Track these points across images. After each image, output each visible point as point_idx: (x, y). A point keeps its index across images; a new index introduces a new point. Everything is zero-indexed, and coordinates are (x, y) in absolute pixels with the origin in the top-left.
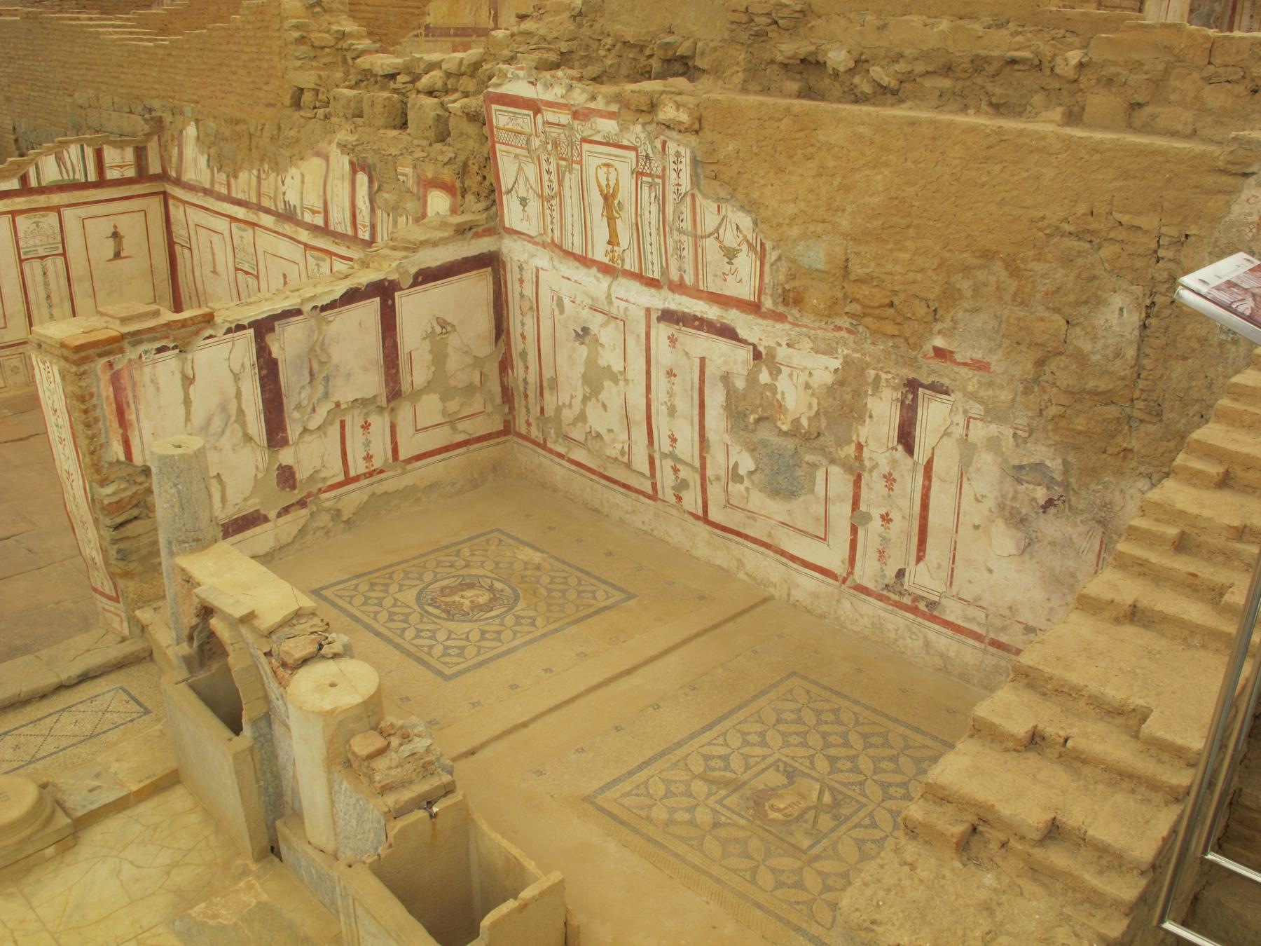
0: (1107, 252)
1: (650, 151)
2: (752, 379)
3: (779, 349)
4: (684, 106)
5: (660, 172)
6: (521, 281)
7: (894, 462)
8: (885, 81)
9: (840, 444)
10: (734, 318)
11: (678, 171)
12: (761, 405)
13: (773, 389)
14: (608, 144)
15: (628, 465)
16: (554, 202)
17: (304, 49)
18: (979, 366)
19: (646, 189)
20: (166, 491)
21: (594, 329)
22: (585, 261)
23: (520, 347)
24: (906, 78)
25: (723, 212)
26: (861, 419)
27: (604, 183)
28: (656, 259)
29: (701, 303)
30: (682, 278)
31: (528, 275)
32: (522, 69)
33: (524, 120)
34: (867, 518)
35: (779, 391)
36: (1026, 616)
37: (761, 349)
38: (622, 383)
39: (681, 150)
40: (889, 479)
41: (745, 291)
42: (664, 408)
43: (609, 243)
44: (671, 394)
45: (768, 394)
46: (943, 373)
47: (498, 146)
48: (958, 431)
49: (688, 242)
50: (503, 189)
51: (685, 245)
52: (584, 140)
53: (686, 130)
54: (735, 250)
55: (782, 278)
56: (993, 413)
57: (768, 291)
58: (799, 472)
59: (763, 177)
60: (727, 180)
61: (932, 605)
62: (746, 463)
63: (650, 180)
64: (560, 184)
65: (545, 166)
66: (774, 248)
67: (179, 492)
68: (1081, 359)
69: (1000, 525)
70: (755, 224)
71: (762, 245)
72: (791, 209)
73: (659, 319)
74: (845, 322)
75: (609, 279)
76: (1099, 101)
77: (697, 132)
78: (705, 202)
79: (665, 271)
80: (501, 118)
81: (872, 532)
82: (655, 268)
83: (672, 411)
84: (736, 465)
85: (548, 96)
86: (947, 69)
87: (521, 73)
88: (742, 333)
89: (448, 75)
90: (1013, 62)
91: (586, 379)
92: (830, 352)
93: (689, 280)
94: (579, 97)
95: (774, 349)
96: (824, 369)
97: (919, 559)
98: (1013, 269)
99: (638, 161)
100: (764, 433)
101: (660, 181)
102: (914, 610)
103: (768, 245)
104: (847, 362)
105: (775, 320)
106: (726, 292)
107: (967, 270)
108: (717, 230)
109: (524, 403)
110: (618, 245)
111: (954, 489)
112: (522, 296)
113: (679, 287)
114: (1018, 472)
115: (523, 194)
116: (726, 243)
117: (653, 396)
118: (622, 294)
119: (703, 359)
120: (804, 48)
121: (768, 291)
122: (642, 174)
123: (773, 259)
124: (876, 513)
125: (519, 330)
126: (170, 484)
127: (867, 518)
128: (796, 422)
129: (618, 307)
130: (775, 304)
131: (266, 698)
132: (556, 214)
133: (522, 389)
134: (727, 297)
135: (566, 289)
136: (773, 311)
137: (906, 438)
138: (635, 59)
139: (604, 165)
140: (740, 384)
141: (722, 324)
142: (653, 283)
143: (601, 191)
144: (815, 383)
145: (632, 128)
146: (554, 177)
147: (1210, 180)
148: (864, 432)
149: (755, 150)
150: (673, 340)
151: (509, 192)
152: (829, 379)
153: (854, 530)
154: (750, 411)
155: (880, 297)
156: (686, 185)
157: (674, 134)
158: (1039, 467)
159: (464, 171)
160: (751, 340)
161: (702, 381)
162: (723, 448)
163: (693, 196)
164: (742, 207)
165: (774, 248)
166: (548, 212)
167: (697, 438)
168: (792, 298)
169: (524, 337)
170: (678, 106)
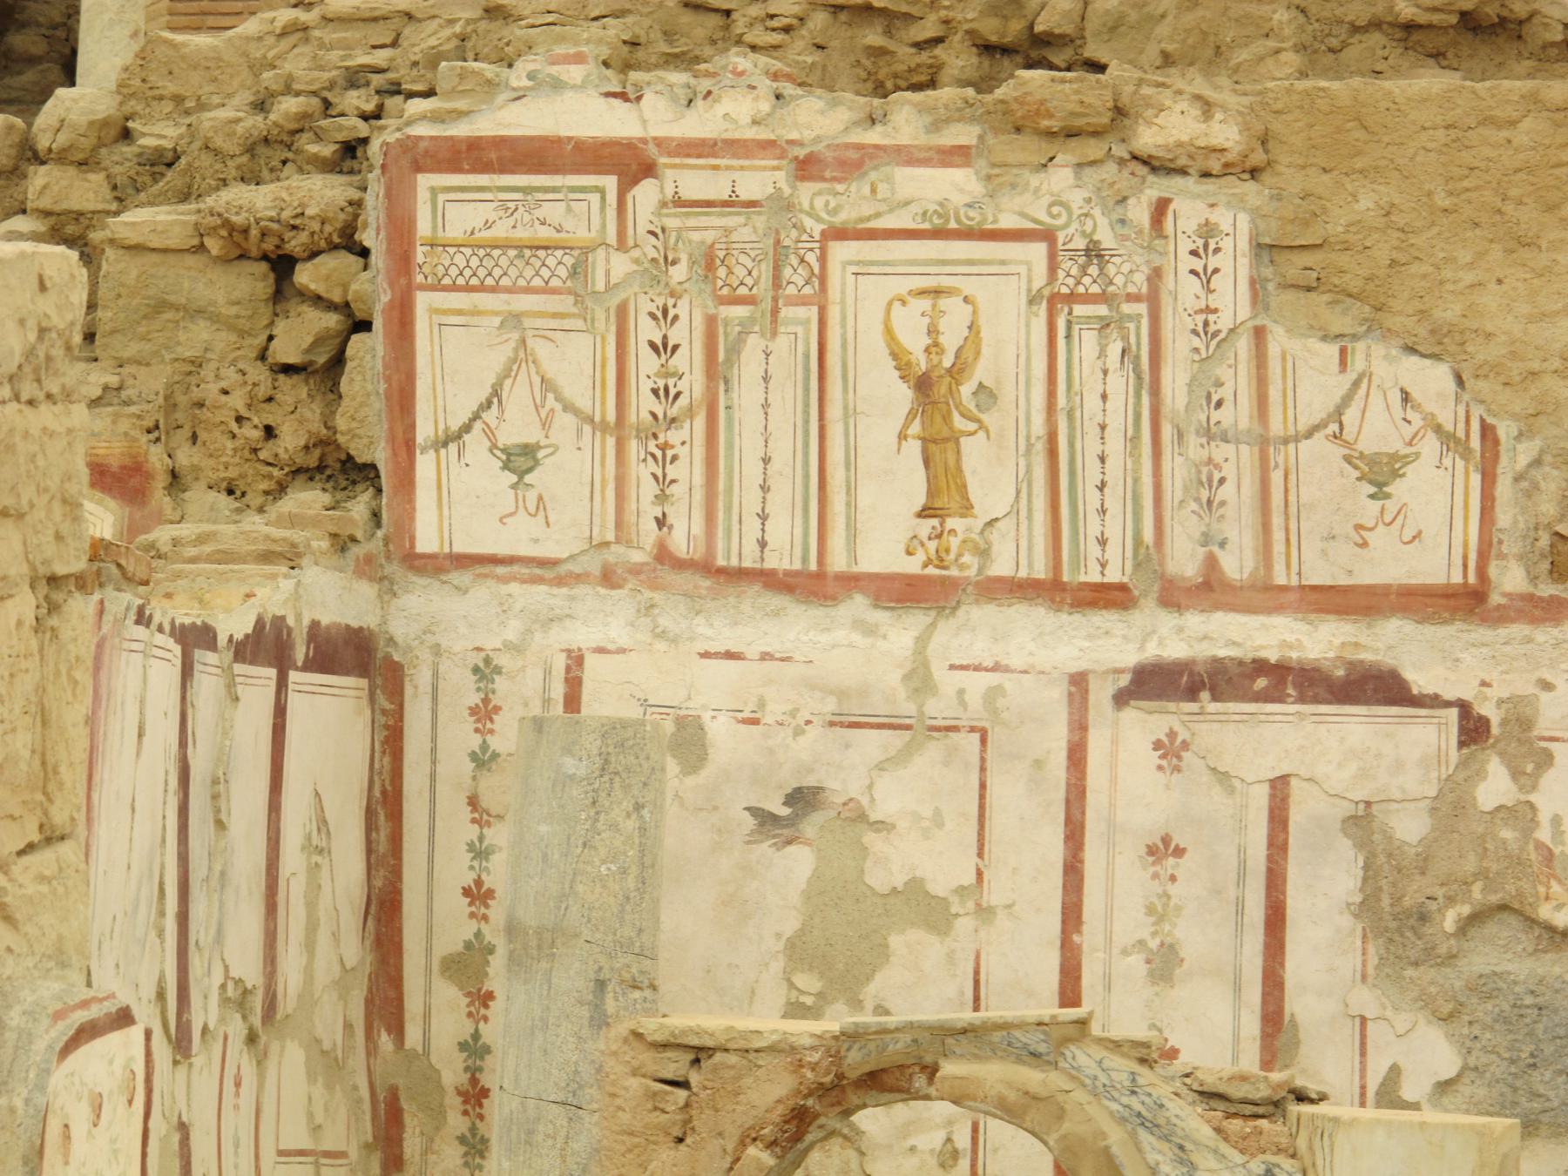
1: (1106, 238)
3: (1545, 697)
4: (1225, 109)
5: (1140, 282)
6: (484, 713)
10: (1394, 643)
11: (1206, 277)
12: (1482, 874)
13: (1522, 815)
14: (938, 234)
16: (674, 436)
19: (1088, 341)
20: (614, 827)
22: (813, 585)
25: (1358, 364)
27: (914, 342)
29: (1279, 621)
30: (1211, 563)
31: (525, 690)
32: (579, 59)
33: (576, 208)
35: (1544, 817)
37: (1487, 710)
38: (964, 925)
39: (1232, 218)
41: (1436, 564)
42: (1136, 962)
43: (925, 512)
44: (1159, 913)
45: (1507, 834)
47: (422, 301)
49: (1237, 462)
50: (424, 430)
51: (1229, 471)
52: (841, 234)
53: (1228, 169)
54: (1394, 457)
55: (1548, 508)
57: (1511, 547)
59: (1471, 266)
60: (1354, 285)
62: (1430, 1054)
63: (1102, 310)
64: (716, 371)
66: (1520, 436)
67: (643, 830)
70: (1460, 381)
71: (1487, 431)
73: (1122, 699)
75: (916, 620)
77: (1254, 173)
78: (1295, 346)
79: (1147, 555)
80: (451, 210)
82: (1113, 552)
83: (1164, 964)
84: (1394, 1072)
85: (699, 124)
87: (575, 73)
88: (1420, 680)
91: (798, 951)
93: (1236, 564)
94: (820, 119)
95: (1530, 700)
99: (1053, 267)
101: (1142, 308)
103: (1505, 430)
105: (1534, 621)
106: (1368, 576)
108: (1338, 414)
109: (456, 1122)
110: (967, 509)
113: (1209, 589)
116: (1368, 445)
117: (1090, 937)
118: (979, 648)
119: (1280, 788)
121: (1511, 547)
122: (1072, 298)
123: (1523, 460)
125: (456, 871)
126: (628, 805)
130: (1533, 579)
132: (687, 471)
134: (1370, 590)
135: (711, 692)
136: (1530, 598)
138: (878, 53)
139: (922, 293)
140: (1410, 827)
141: (1351, 665)
142: (1109, 597)
143: (903, 365)
145: (1034, 180)
149: (1442, 200)
150: (1170, 751)
151: (454, 438)
156: (1232, 301)
157: (1190, 183)
159: (177, 417)
160: (1449, 695)
161: (1278, 846)
162: (1350, 1031)
163: (1259, 334)
164: (1411, 350)
165: (1520, 436)
166: (642, 474)
167: (1251, 1025)
169: (477, 894)
170: (1207, 107)
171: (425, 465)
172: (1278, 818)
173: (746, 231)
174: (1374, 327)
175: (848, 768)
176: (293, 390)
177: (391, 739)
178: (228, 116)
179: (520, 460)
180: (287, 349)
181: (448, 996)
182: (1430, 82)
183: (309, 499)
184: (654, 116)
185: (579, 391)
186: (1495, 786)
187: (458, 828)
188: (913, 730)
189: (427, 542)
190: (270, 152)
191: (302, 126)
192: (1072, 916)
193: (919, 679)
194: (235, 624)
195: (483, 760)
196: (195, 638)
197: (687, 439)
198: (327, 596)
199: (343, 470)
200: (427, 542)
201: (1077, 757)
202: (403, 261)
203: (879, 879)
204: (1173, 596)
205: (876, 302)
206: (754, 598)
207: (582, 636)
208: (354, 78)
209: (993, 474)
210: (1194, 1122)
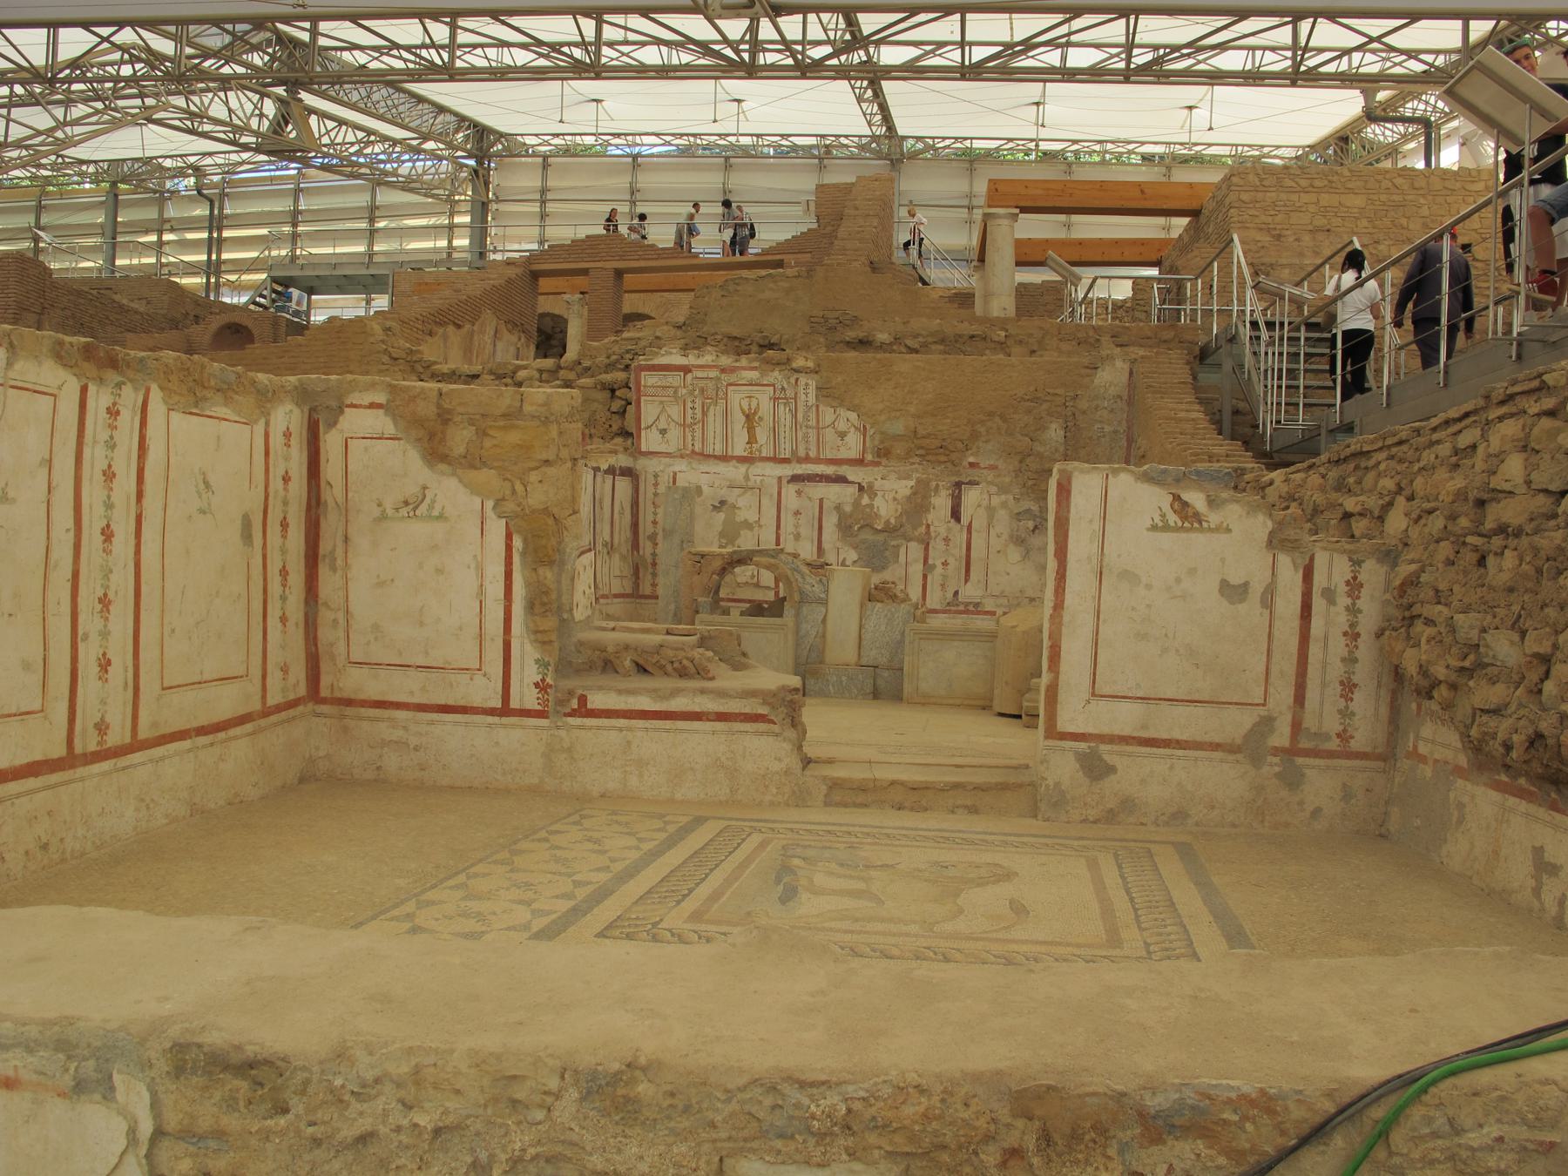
0: (1045, 406)
2: (856, 504)
6: (656, 485)
7: (949, 530)
8: (916, 346)
9: (915, 528)
13: (871, 506)
15: (757, 585)
17: (386, 359)
18: (993, 468)
21: (731, 500)
22: (724, 458)
23: (650, 530)
24: (925, 345)
26: (928, 511)
27: (746, 408)
28: (788, 446)
31: (665, 480)
33: (674, 379)
34: (934, 567)
36: (1029, 593)
40: (947, 540)
41: (853, 454)
46: (974, 474)
48: (985, 503)
49: (812, 434)
56: (1003, 490)
58: (887, 553)
61: (977, 605)
62: (852, 555)
64: (704, 413)
65: (689, 405)
68: (1040, 456)
69: (1011, 546)
72: (881, 406)
74: (917, 460)
76: (1016, 350)
79: (794, 452)
80: (649, 379)
81: (935, 578)
83: (797, 537)
85: (700, 362)
86: (943, 341)
88: (850, 478)
89: (541, 371)
90: (972, 337)
91: (722, 535)
92: (908, 477)
93: (812, 454)
94: (726, 361)
96: (904, 488)
97: (966, 581)
98: (1005, 420)
100: (867, 535)
102: (966, 612)
104: (919, 481)
107: (982, 422)
111: (985, 535)
112: (656, 494)
113: (807, 459)
114: (1018, 516)
115: (662, 425)
117: (782, 531)
118: (759, 471)
119: (821, 501)
120: (861, 335)
124: (938, 563)
125: (650, 518)
127: (934, 567)
128: (888, 522)
129: (755, 480)
131: (801, 593)
132: (698, 434)
133: (649, 560)
135: (704, 481)
137: (956, 514)
140: (848, 509)
142: (785, 461)
144: (899, 496)
146: (699, 411)
147: (1084, 371)
148: (931, 517)
150: (799, 493)
152: (908, 492)
153: (925, 577)
154: (853, 525)
155: (938, 443)
156: (812, 399)
158: (1028, 511)
161: (821, 512)
166: (689, 435)
168: (883, 453)
169: (655, 523)
171: (643, 433)
172: (821, 507)
173: (710, 384)
174: (841, 405)
175: (732, 496)
176: (615, 417)
177: (636, 490)
178: (602, 359)
179: (663, 432)
180: (614, 409)
181: (649, 544)
182: (852, 354)
183: (619, 440)
184: (691, 360)
185: (675, 418)
186: (865, 500)
187: (651, 509)
188: (746, 489)
189: (644, 449)
190: (610, 367)
191: (617, 361)
192: (778, 527)
193: (747, 478)
194: (604, 467)
195: (656, 494)
196: (596, 469)
197: (698, 427)
198: (623, 460)
199: (627, 434)
200: (644, 449)
201: (779, 494)
202: (639, 390)
203: (738, 519)
204: (800, 461)
205: (737, 398)
206: (712, 461)
207: (676, 469)
208: (628, 352)
209: (762, 435)
210: (805, 570)
